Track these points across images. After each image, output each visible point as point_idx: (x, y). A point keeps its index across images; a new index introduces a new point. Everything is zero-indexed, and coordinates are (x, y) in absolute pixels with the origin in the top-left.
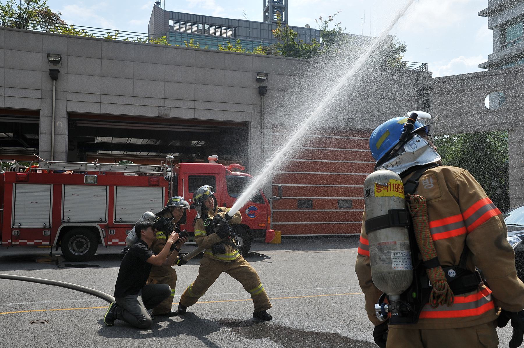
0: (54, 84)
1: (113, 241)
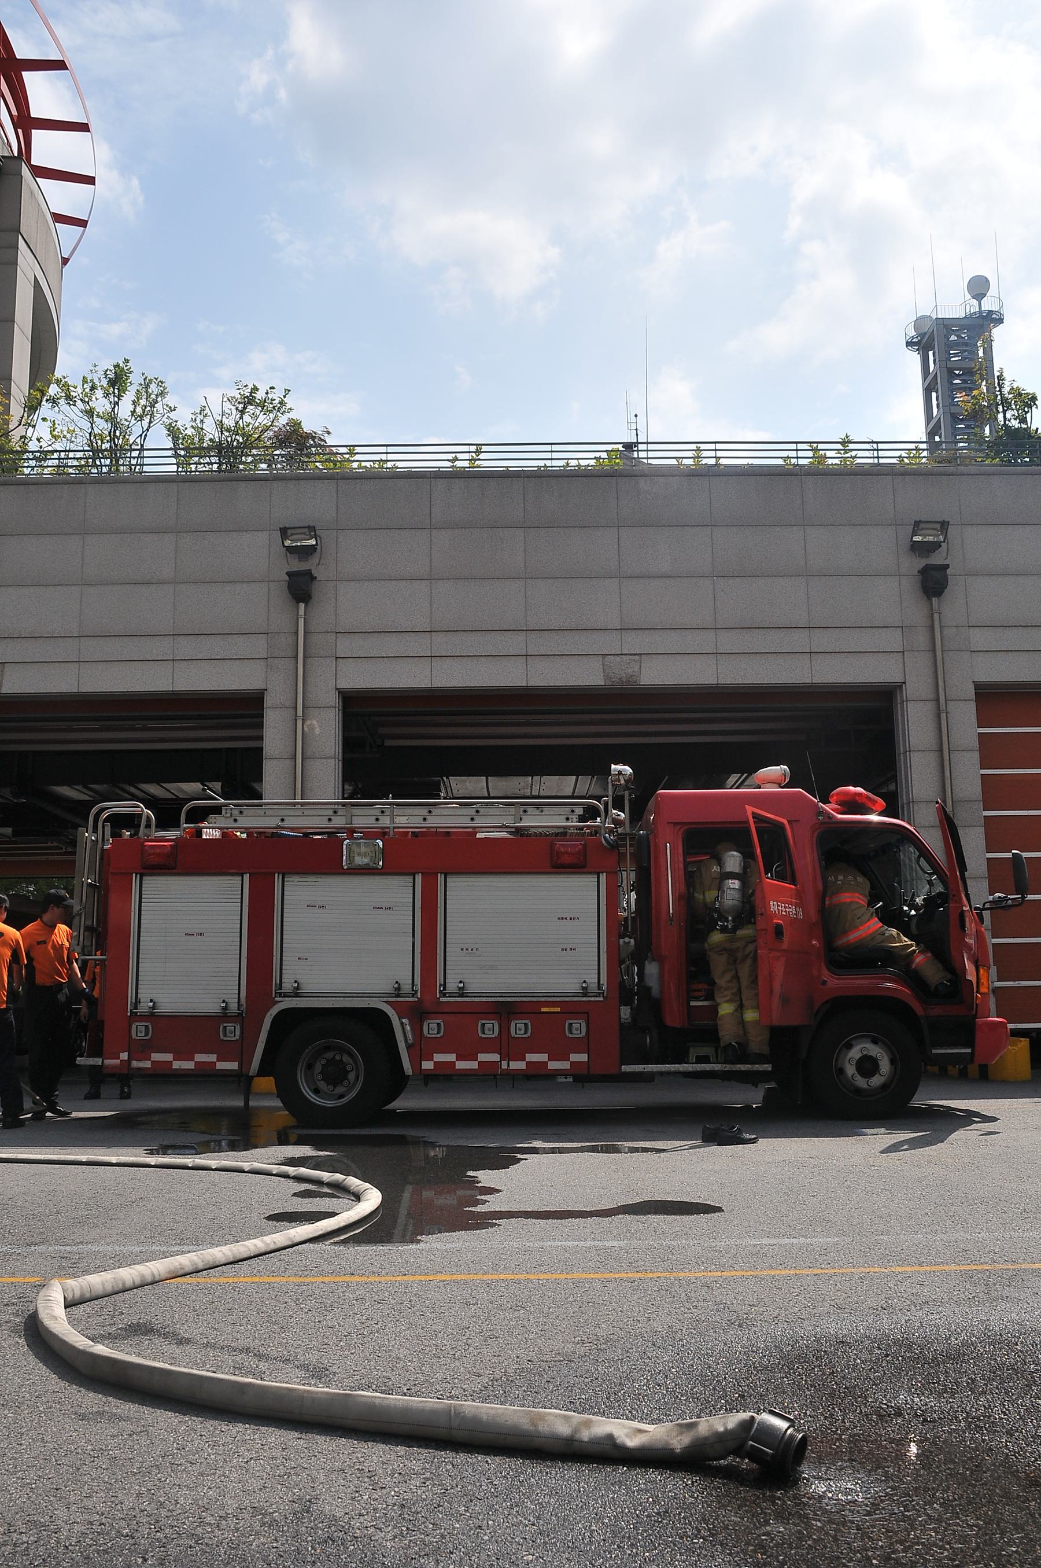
0: (302, 612)
1: (439, 1057)
